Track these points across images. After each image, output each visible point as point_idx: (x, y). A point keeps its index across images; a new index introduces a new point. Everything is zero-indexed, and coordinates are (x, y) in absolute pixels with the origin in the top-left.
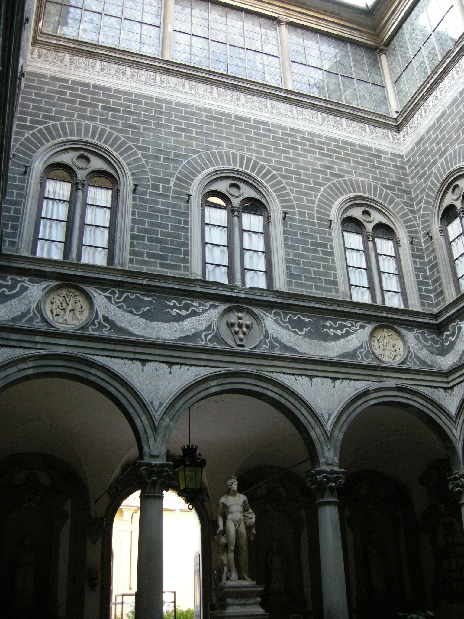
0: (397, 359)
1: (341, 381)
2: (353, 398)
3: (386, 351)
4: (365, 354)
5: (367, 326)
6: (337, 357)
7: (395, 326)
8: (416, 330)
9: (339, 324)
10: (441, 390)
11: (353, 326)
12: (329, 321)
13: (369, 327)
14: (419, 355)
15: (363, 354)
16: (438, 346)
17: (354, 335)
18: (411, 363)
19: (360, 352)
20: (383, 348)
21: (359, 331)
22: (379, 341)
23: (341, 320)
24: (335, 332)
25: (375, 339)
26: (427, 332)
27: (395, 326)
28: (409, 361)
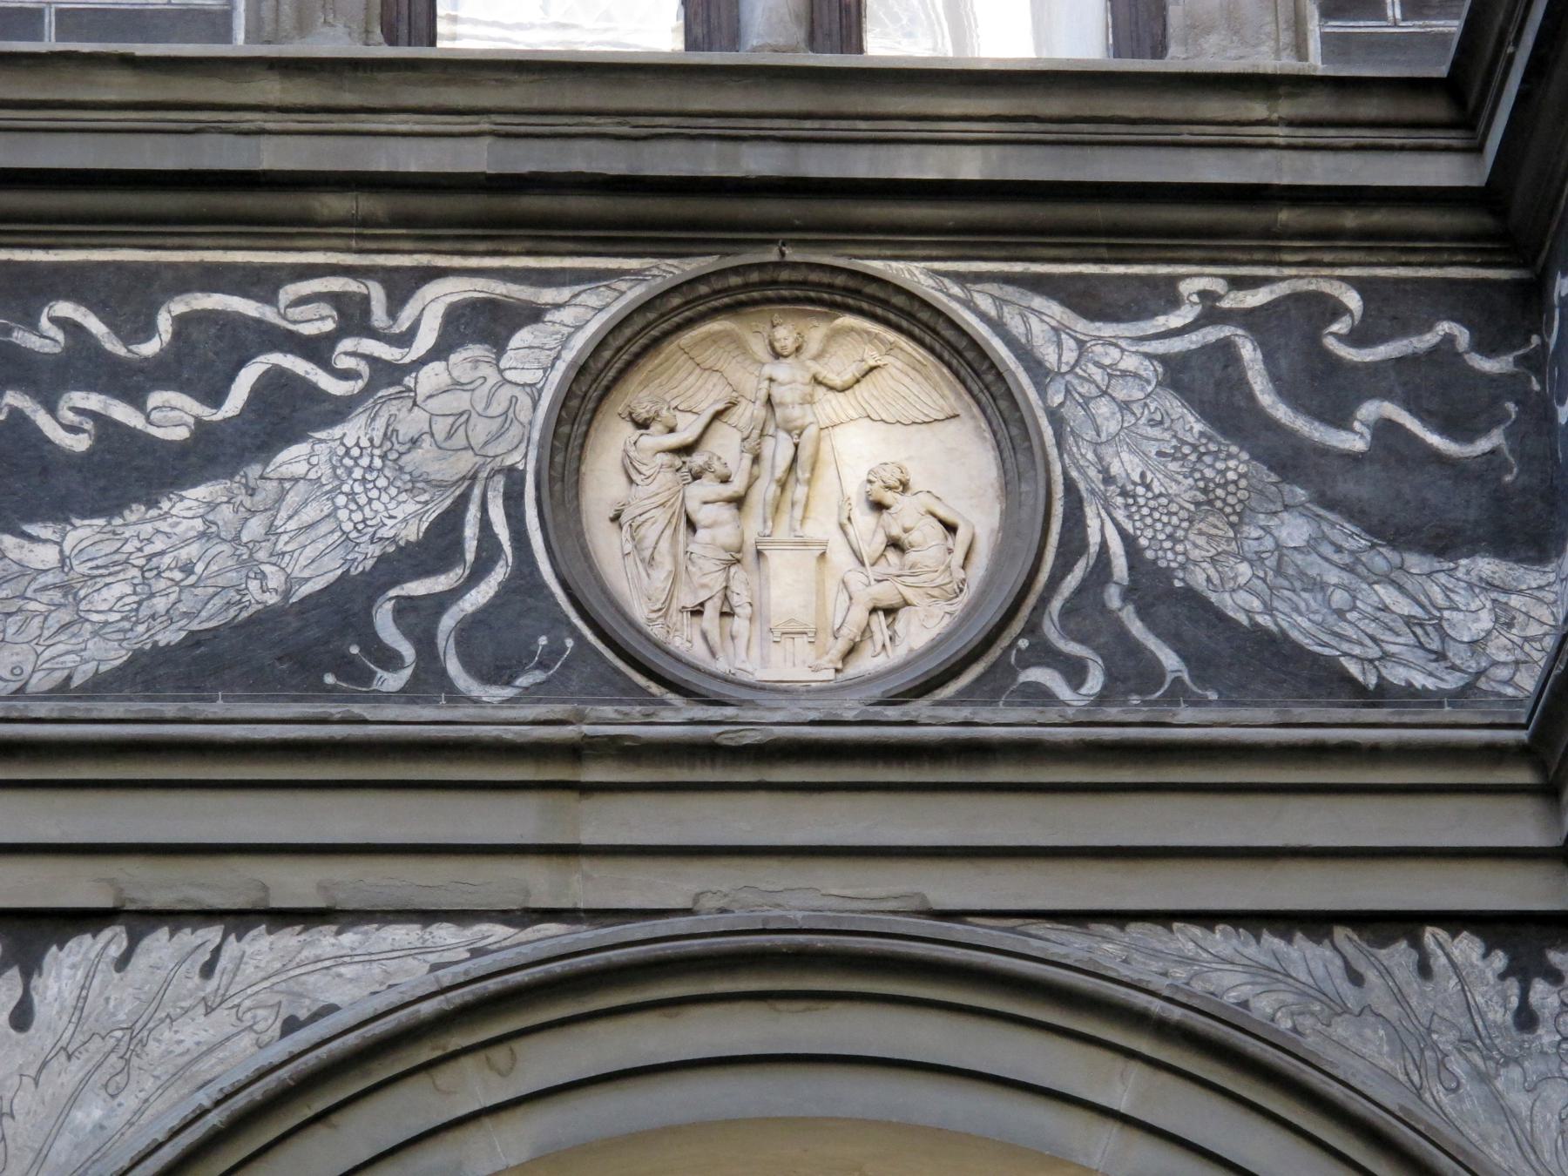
0: (898, 654)
1: (115, 951)
2: (215, 1119)
3: (775, 558)
4: (468, 630)
5: (535, 314)
6: (100, 686)
7: (912, 274)
8: (1196, 281)
9: (181, 322)
10: (1467, 947)
11: (353, 317)
12: (64, 309)
13: (567, 315)
14: (1198, 579)
15: (448, 622)
16: (1493, 440)
17: (353, 430)
18: (1074, 672)
19: (405, 608)
20: (726, 535)
21: (431, 377)
22: (697, 460)
23: (213, 278)
24: (122, 412)
25: (656, 439)
26: (1353, 300)
27: (912, 274)
28: (1046, 655)
